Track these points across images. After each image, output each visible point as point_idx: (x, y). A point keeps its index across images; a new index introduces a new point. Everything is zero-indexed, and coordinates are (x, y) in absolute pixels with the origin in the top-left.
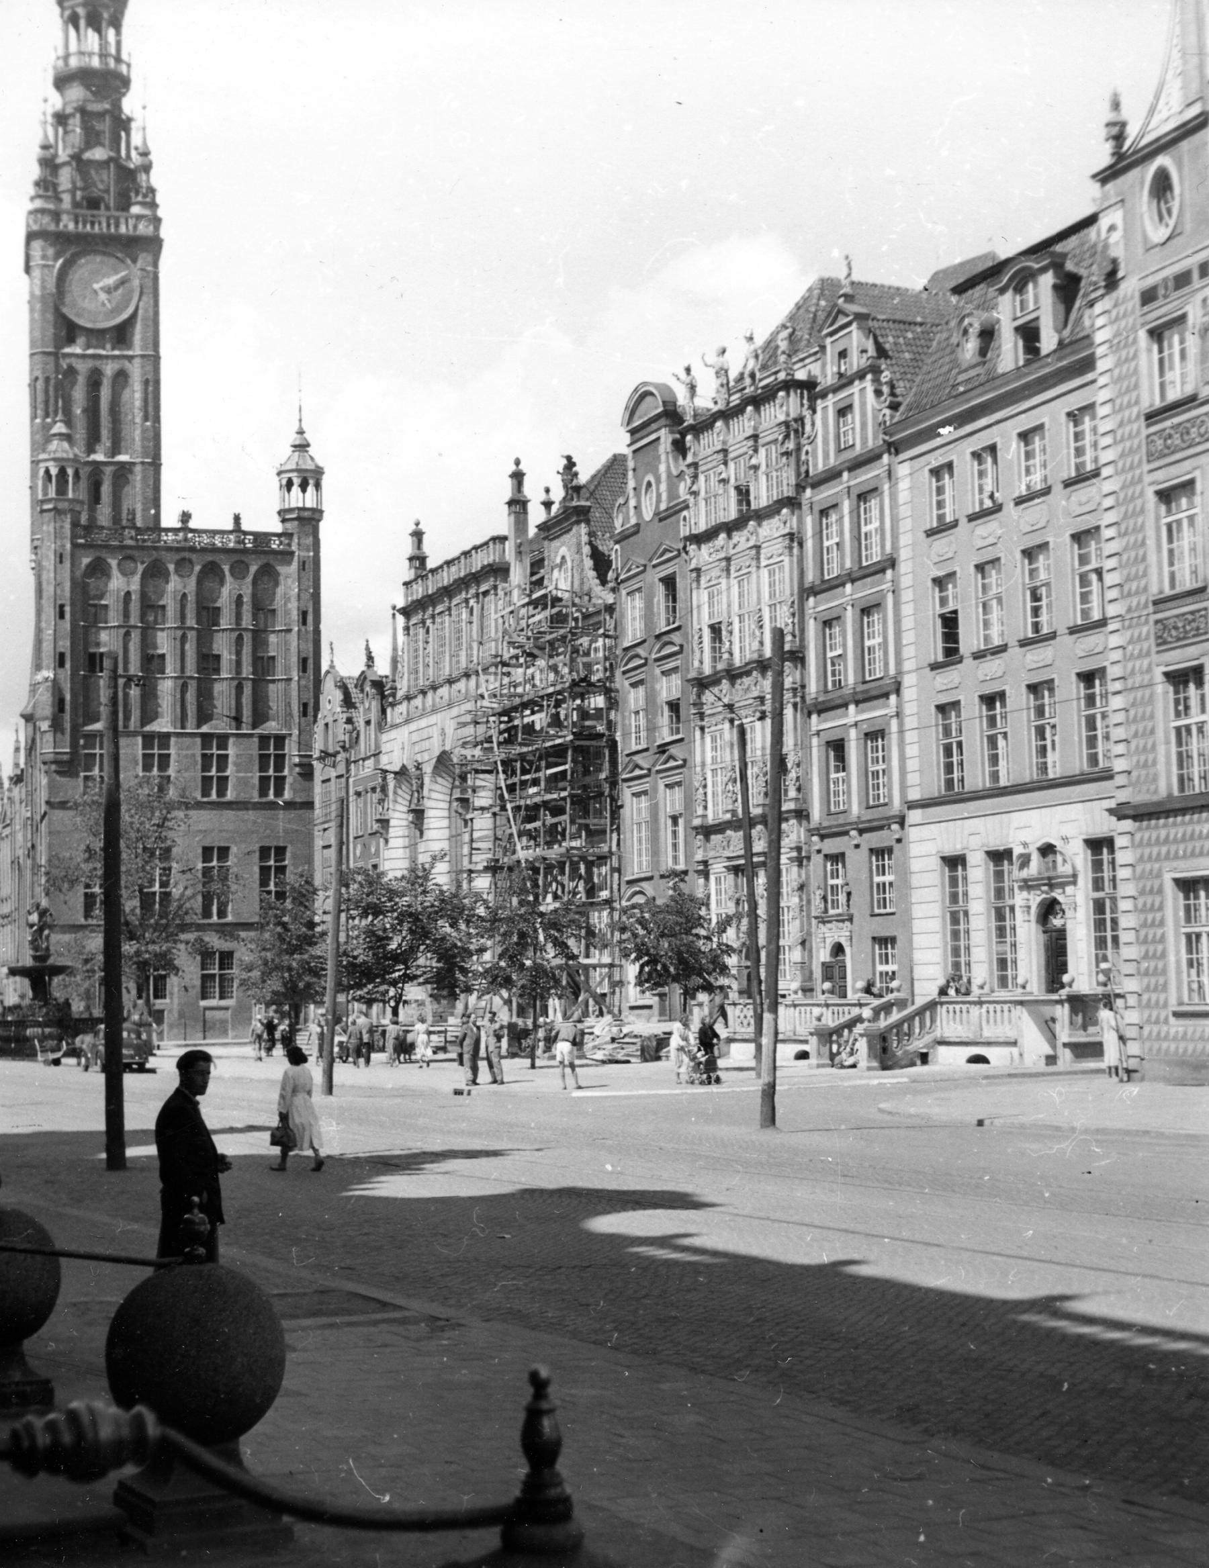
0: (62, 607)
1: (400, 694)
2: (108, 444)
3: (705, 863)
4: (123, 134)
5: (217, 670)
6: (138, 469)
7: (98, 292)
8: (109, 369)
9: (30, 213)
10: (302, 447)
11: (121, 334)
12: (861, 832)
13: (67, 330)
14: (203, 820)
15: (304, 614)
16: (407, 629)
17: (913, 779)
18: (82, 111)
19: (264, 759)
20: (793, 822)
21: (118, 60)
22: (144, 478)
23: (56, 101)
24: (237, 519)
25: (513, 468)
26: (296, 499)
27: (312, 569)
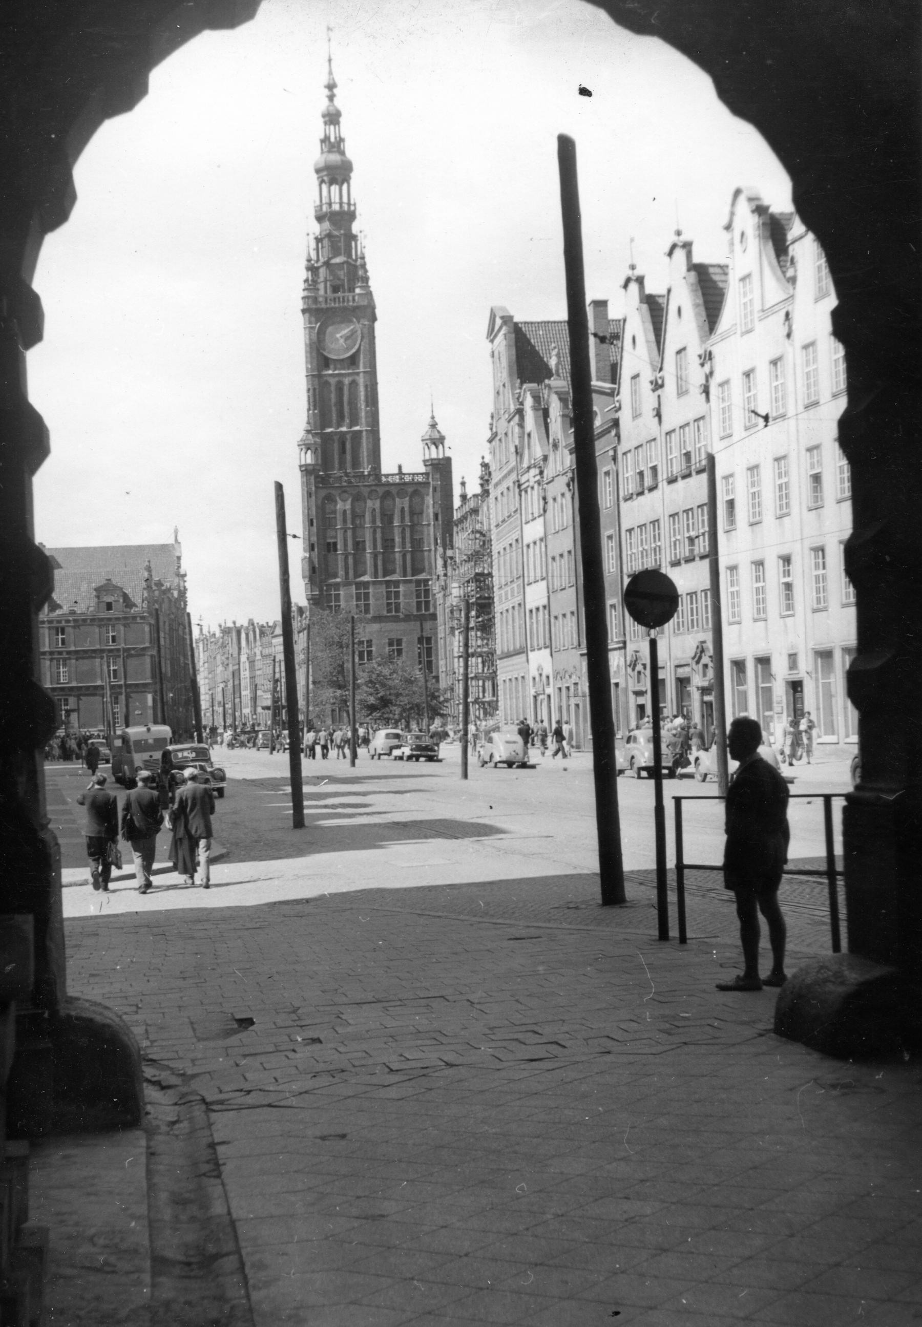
4: (353, 243)
5: (393, 547)
6: (364, 433)
7: (339, 339)
8: (347, 381)
9: (303, 298)
18: (329, 236)
21: (349, 204)
22: (367, 438)
23: (316, 228)
24: (400, 467)
26: (434, 453)
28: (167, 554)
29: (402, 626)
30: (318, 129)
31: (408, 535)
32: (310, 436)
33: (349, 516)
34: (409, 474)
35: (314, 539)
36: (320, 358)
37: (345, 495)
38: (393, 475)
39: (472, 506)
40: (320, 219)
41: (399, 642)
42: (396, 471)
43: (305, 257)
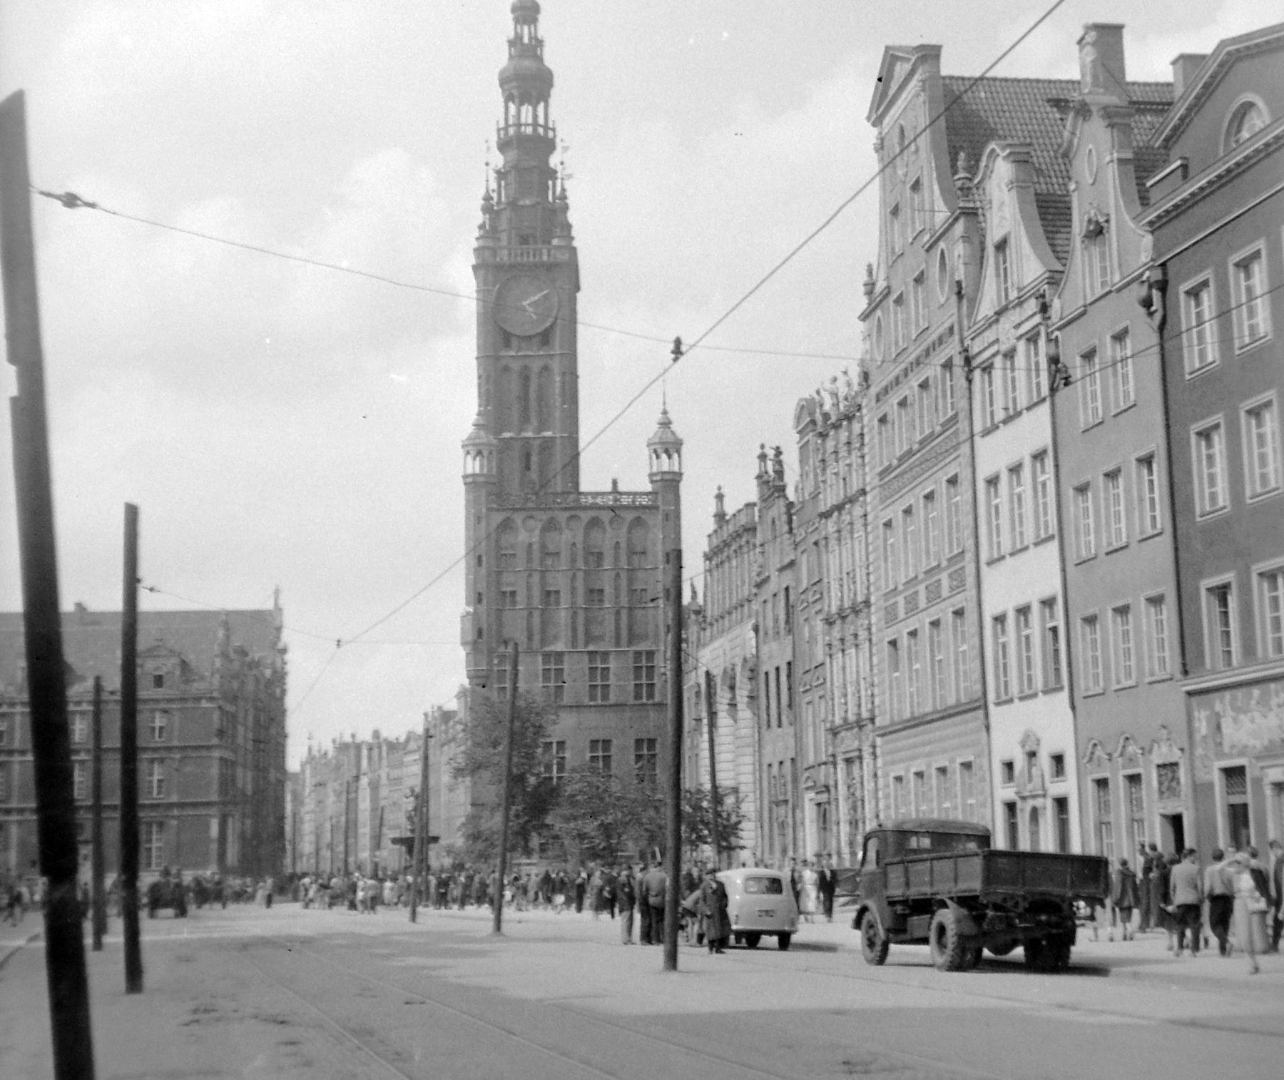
0: (479, 558)
1: (709, 620)
2: (535, 424)
3: (834, 756)
4: (550, 183)
5: (601, 601)
6: (558, 441)
8: (536, 366)
9: (475, 250)
11: (545, 338)
13: (507, 338)
14: (591, 718)
19: (638, 669)
21: (546, 127)
23: (498, 160)
24: (615, 483)
26: (665, 464)
27: (673, 518)
28: (266, 624)
29: (611, 719)
30: (508, 28)
31: (624, 583)
32: (482, 433)
33: (536, 555)
34: (628, 494)
35: (482, 587)
36: (499, 335)
37: (531, 523)
38: (603, 494)
39: (743, 522)
40: (503, 146)
41: (607, 743)
42: (609, 488)
43: (482, 192)
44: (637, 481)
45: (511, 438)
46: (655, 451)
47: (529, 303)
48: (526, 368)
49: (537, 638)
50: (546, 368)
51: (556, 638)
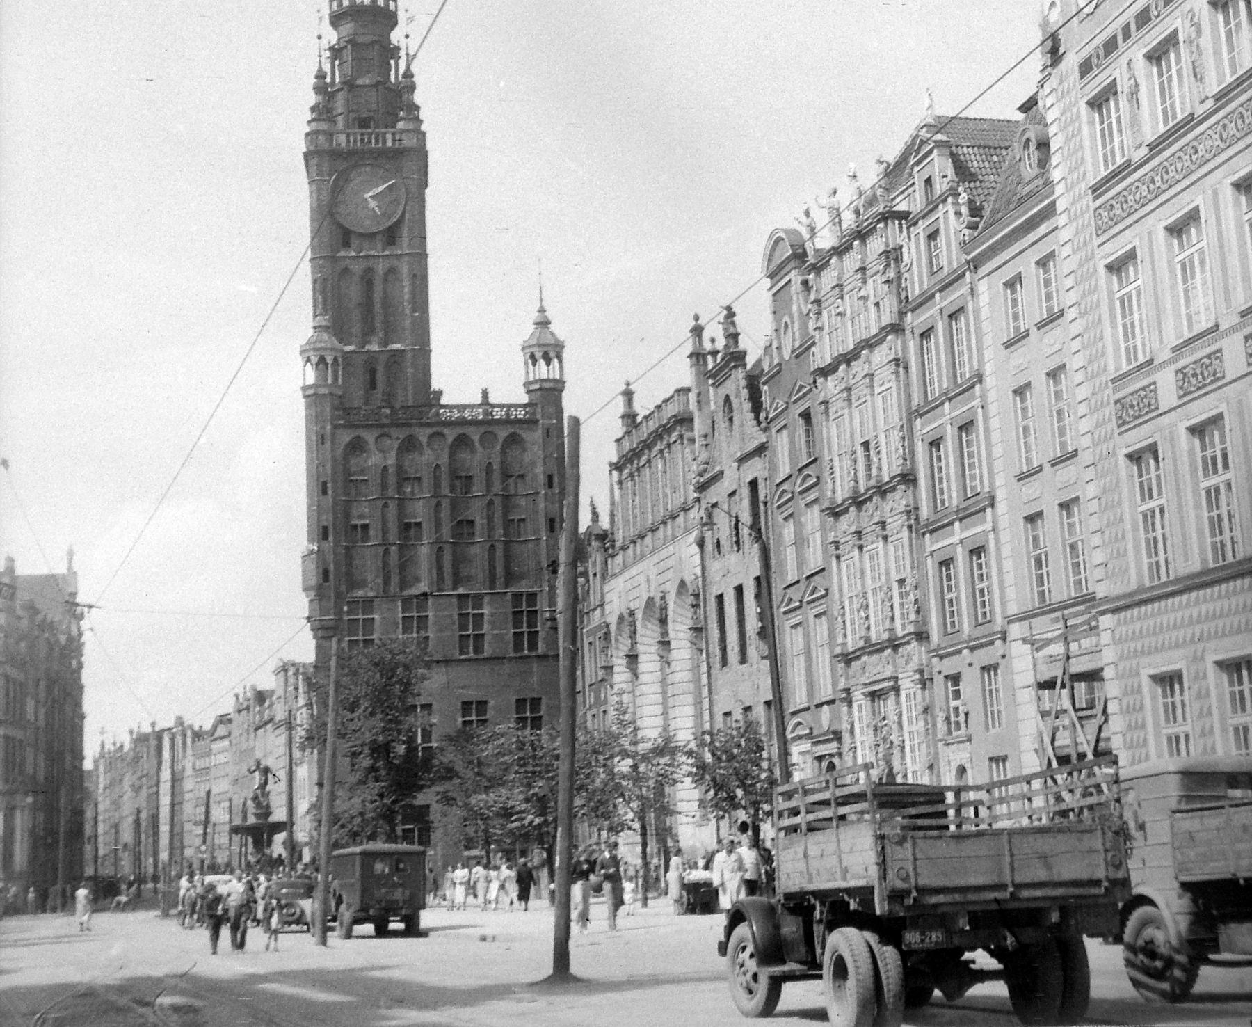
0: (325, 484)
1: (618, 544)
2: (381, 334)
3: (848, 690)
4: (392, 62)
5: (472, 535)
6: (409, 355)
8: (380, 268)
9: (307, 135)
10: (544, 324)
11: (391, 236)
12: (972, 649)
13: (345, 236)
14: (460, 674)
15: (550, 478)
16: (620, 483)
17: (1011, 593)
18: (352, 42)
20: (914, 644)
23: (331, 36)
24: (485, 393)
25: (693, 323)
26: (542, 371)
32: (325, 336)
33: (392, 480)
34: (501, 406)
35: (328, 519)
36: (335, 234)
37: (387, 442)
40: (336, 20)
41: (482, 705)
42: (479, 400)
44: (510, 390)
45: (353, 352)
46: (533, 357)
47: (371, 197)
48: (369, 270)
49: (395, 579)
50: (392, 271)
51: (417, 580)
